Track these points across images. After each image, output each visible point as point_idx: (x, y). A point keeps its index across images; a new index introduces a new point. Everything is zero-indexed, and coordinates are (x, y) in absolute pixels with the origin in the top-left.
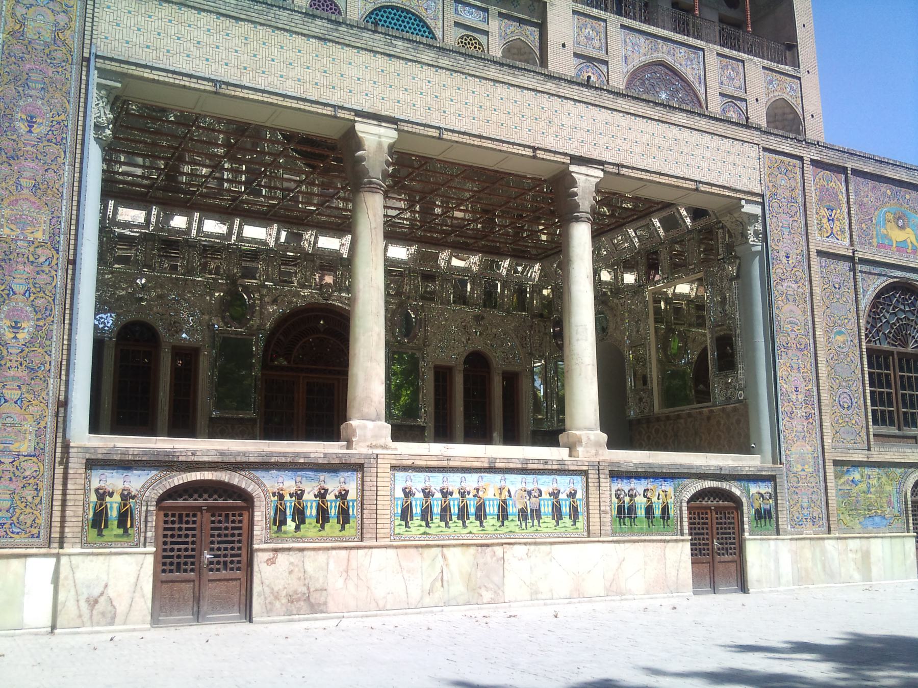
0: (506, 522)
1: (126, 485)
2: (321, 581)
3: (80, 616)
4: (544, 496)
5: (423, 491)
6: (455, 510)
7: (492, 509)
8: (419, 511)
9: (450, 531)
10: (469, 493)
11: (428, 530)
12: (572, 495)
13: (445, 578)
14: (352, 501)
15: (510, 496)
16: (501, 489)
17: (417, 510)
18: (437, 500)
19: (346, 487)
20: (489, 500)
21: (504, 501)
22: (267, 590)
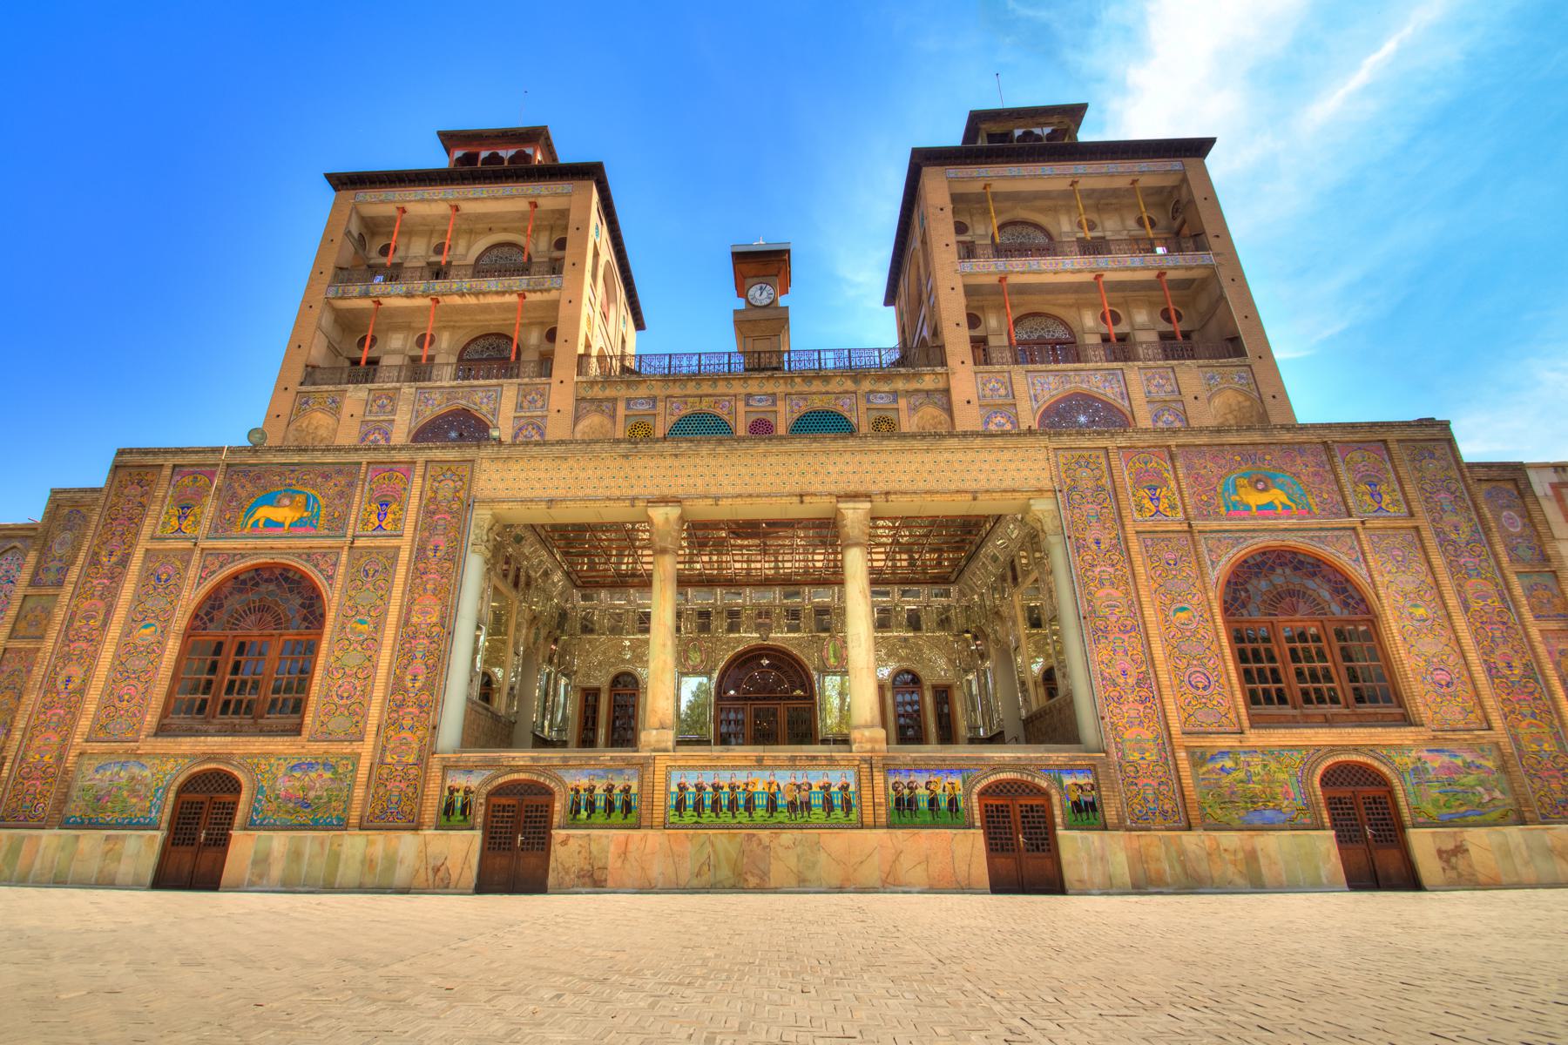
0: (775, 814)
1: (469, 784)
2: (603, 861)
3: (427, 880)
4: (814, 789)
5: (696, 786)
6: (725, 802)
7: (761, 801)
8: (691, 802)
9: (721, 820)
10: (739, 787)
11: (699, 820)
12: (845, 788)
13: (712, 863)
14: (635, 794)
15: (779, 789)
16: (770, 784)
17: (690, 802)
18: (709, 793)
19: (629, 783)
20: (759, 793)
21: (774, 795)
22: (560, 867)
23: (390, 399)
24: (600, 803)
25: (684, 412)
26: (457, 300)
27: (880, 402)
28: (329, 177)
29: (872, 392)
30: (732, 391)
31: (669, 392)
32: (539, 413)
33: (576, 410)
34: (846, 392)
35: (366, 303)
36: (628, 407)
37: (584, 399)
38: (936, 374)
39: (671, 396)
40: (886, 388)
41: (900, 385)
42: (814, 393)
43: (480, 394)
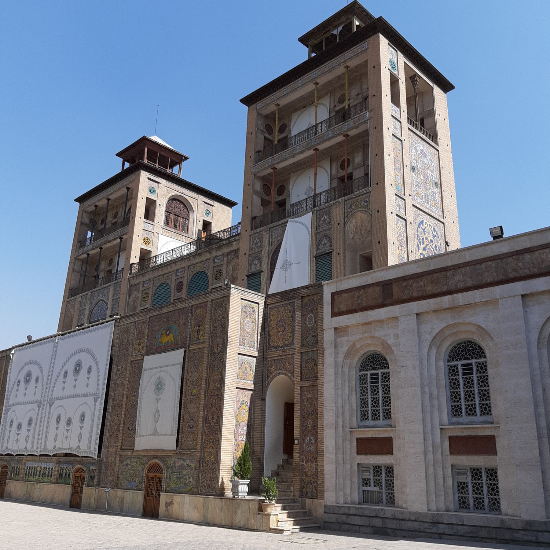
23: (86, 299)
24: (15, 472)
25: (159, 284)
26: (109, 245)
27: (218, 262)
28: (75, 200)
29: (216, 257)
30: (172, 270)
31: (154, 276)
32: (118, 297)
33: (130, 290)
34: (207, 260)
35: (85, 256)
36: (143, 286)
37: (132, 285)
38: (236, 240)
39: (155, 277)
40: (220, 254)
41: (226, 250)
42: (197, 263)
43: (106, 291)
